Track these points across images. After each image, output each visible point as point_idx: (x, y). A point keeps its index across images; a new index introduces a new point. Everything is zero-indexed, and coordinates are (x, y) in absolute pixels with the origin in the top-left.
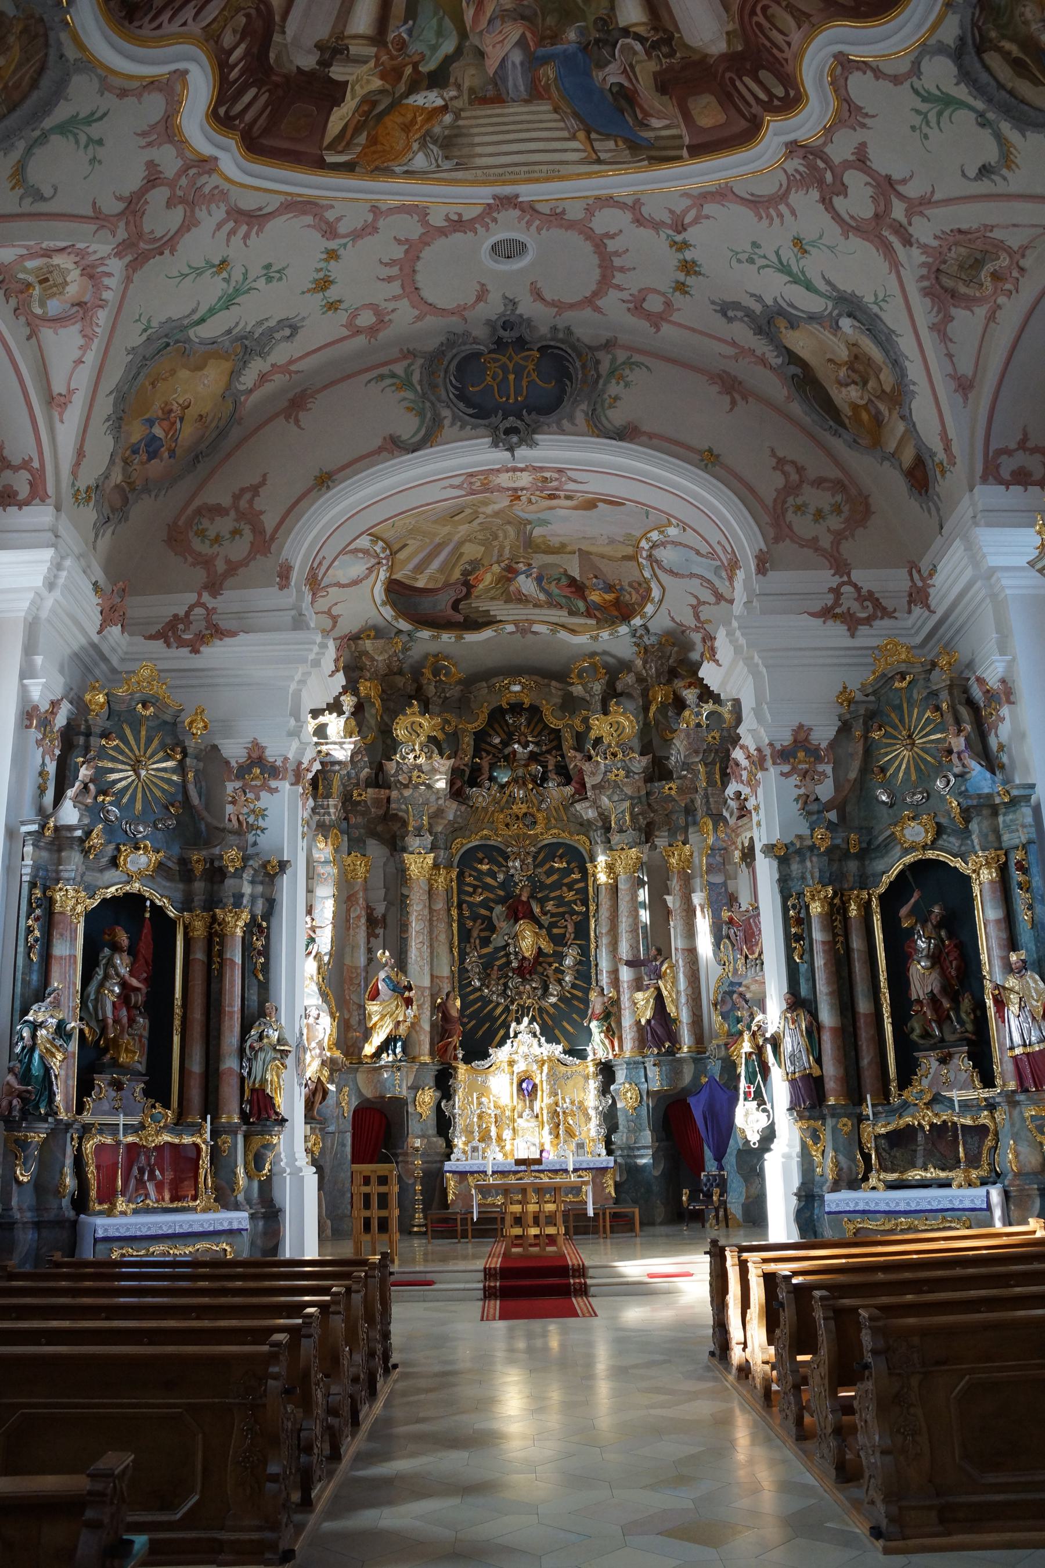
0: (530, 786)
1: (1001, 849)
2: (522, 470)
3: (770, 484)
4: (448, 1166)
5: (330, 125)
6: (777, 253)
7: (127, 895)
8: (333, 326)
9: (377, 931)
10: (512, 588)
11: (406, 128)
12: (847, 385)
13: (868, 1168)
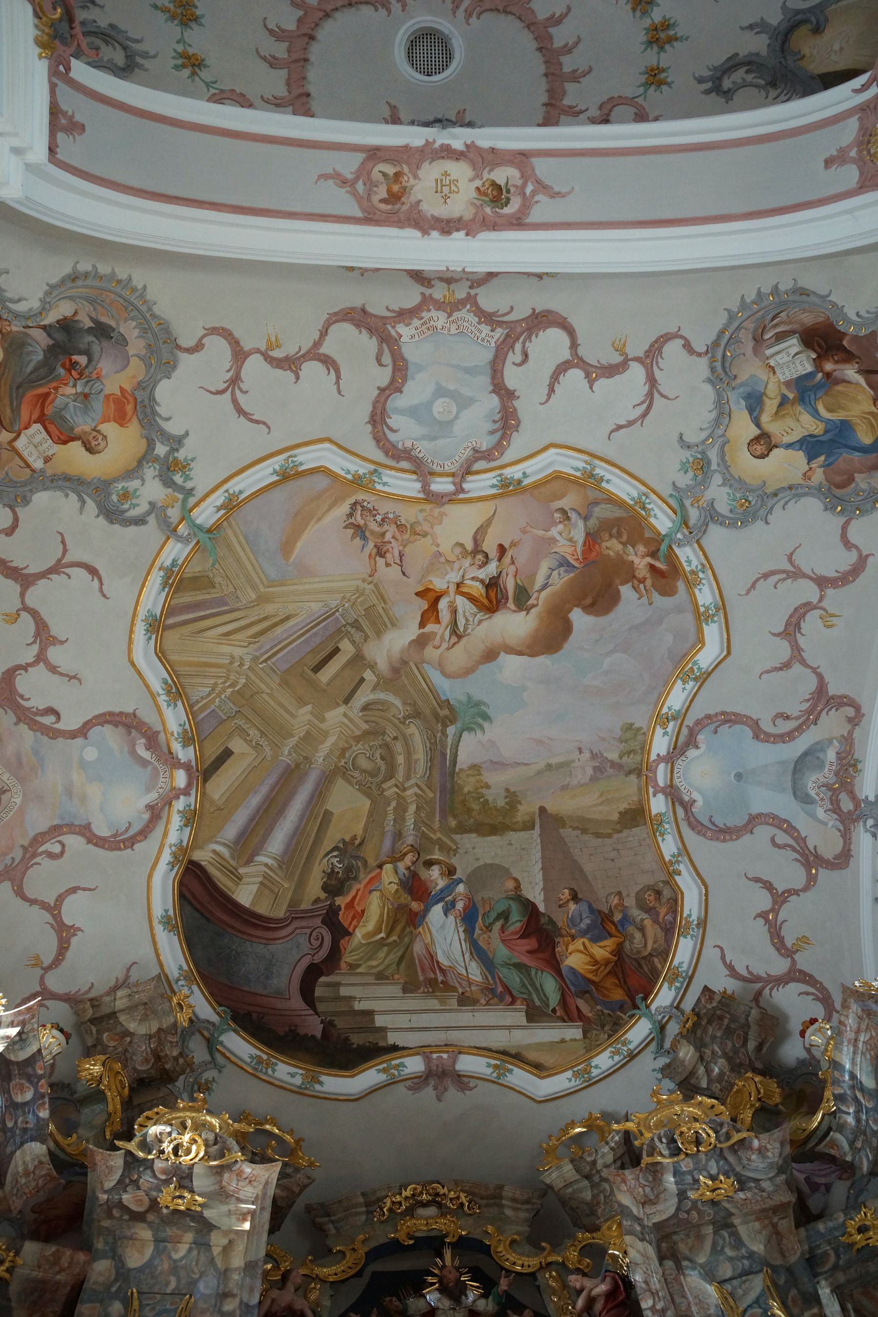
10: (418, 948)
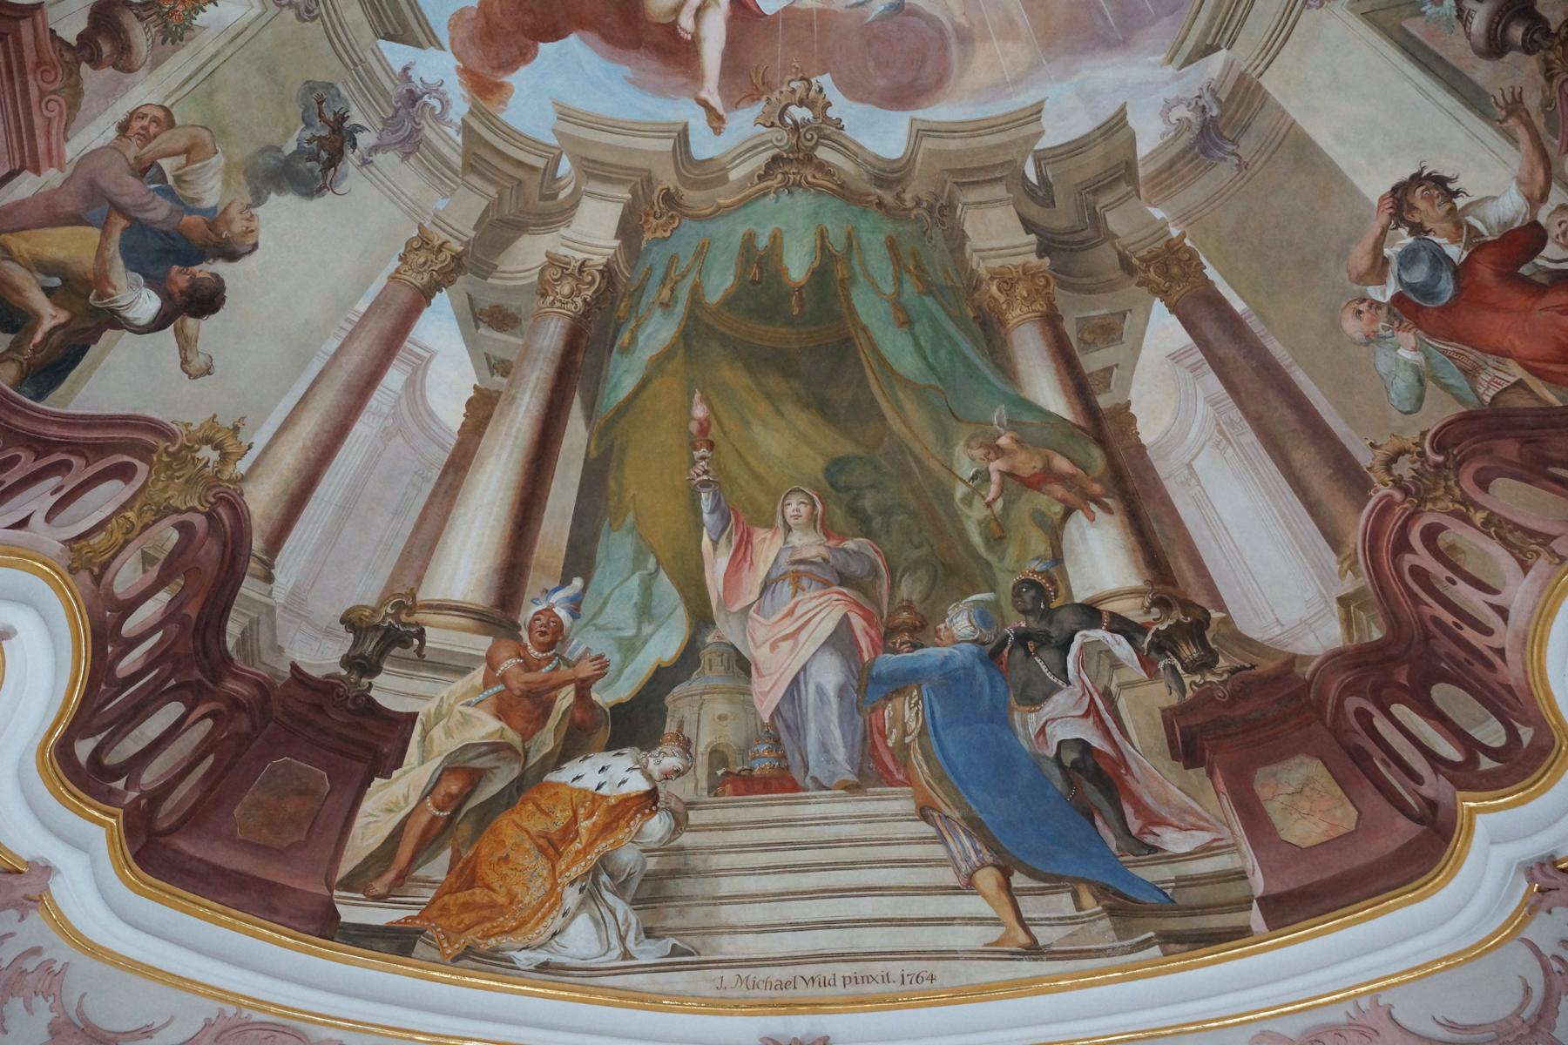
5: (360, 821)
11: (552, 847)
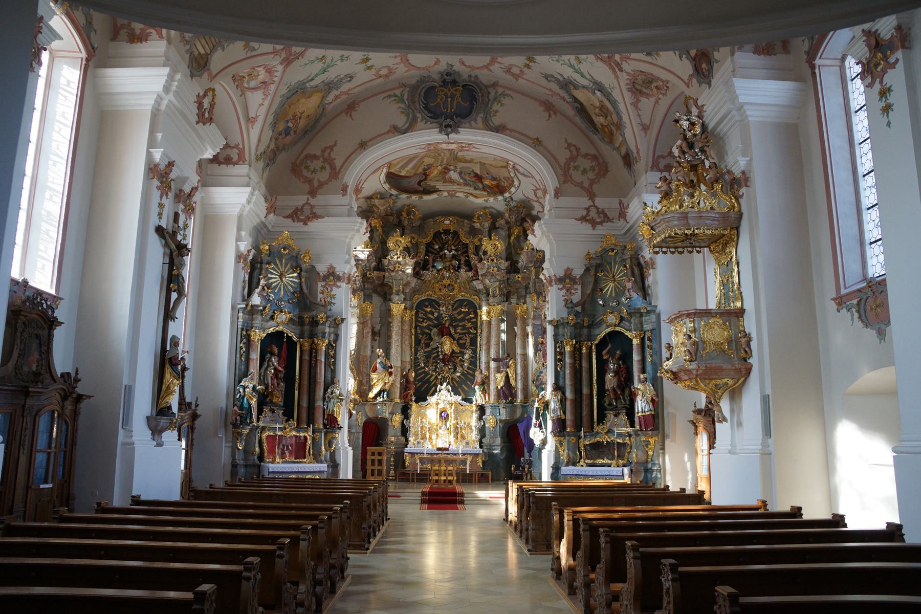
0: (452, 271)
1: (642, 331)
2: (452, 143)
3: (563, 156)
4: (406, 450)
6: (569, 60)
7: (277, 331)
8: (371, 74)
9: (376, 338)
10: (447, 177)
12: (599, 116)
13: (581, 458)
